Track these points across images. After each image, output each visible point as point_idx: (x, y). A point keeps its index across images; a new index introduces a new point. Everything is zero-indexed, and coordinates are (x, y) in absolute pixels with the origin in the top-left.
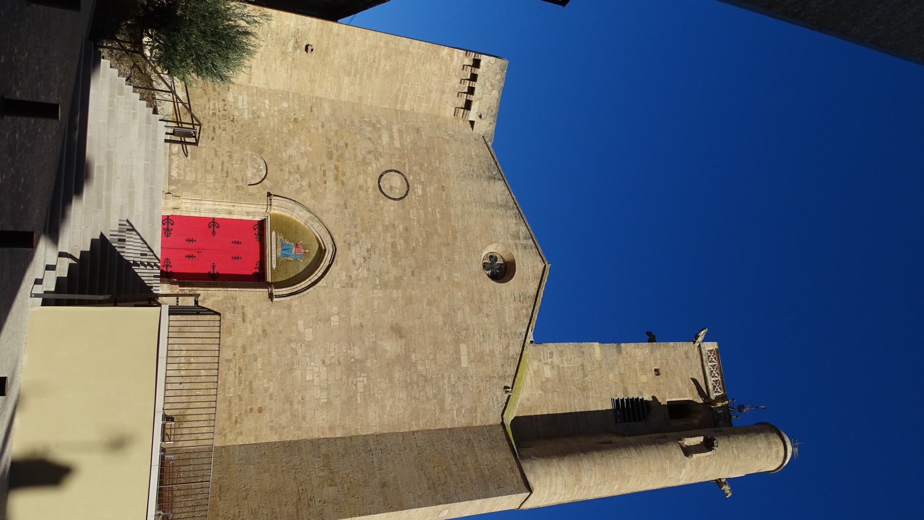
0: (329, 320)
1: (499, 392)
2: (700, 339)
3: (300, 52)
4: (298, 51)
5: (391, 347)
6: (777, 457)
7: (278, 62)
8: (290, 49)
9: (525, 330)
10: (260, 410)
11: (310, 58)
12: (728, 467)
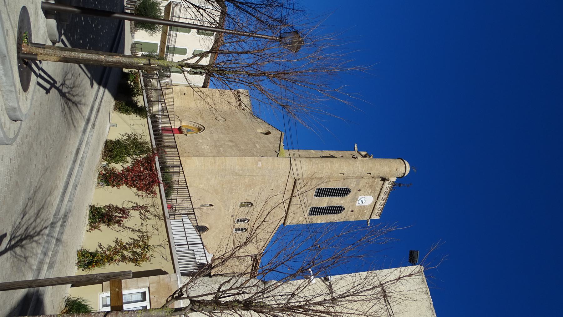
0: (207, 139)
1: (275, 153)
2: (356, 148)
3: (183, 96)
4: (182, 95)
5: (230, 144)
6: (401, 163)
7: (177, 98)
8: (179, 95)
9: (279, 143)
10: (189, 153)
11: (186, 97)
12: (378, 164)
